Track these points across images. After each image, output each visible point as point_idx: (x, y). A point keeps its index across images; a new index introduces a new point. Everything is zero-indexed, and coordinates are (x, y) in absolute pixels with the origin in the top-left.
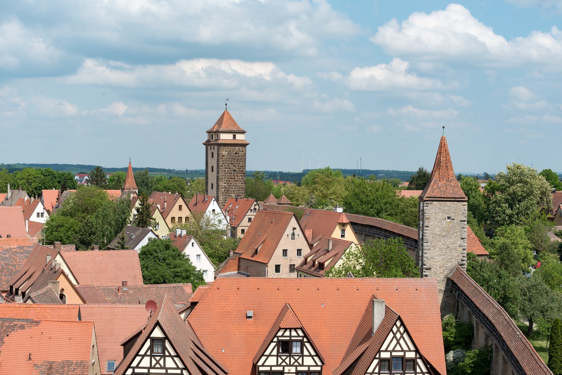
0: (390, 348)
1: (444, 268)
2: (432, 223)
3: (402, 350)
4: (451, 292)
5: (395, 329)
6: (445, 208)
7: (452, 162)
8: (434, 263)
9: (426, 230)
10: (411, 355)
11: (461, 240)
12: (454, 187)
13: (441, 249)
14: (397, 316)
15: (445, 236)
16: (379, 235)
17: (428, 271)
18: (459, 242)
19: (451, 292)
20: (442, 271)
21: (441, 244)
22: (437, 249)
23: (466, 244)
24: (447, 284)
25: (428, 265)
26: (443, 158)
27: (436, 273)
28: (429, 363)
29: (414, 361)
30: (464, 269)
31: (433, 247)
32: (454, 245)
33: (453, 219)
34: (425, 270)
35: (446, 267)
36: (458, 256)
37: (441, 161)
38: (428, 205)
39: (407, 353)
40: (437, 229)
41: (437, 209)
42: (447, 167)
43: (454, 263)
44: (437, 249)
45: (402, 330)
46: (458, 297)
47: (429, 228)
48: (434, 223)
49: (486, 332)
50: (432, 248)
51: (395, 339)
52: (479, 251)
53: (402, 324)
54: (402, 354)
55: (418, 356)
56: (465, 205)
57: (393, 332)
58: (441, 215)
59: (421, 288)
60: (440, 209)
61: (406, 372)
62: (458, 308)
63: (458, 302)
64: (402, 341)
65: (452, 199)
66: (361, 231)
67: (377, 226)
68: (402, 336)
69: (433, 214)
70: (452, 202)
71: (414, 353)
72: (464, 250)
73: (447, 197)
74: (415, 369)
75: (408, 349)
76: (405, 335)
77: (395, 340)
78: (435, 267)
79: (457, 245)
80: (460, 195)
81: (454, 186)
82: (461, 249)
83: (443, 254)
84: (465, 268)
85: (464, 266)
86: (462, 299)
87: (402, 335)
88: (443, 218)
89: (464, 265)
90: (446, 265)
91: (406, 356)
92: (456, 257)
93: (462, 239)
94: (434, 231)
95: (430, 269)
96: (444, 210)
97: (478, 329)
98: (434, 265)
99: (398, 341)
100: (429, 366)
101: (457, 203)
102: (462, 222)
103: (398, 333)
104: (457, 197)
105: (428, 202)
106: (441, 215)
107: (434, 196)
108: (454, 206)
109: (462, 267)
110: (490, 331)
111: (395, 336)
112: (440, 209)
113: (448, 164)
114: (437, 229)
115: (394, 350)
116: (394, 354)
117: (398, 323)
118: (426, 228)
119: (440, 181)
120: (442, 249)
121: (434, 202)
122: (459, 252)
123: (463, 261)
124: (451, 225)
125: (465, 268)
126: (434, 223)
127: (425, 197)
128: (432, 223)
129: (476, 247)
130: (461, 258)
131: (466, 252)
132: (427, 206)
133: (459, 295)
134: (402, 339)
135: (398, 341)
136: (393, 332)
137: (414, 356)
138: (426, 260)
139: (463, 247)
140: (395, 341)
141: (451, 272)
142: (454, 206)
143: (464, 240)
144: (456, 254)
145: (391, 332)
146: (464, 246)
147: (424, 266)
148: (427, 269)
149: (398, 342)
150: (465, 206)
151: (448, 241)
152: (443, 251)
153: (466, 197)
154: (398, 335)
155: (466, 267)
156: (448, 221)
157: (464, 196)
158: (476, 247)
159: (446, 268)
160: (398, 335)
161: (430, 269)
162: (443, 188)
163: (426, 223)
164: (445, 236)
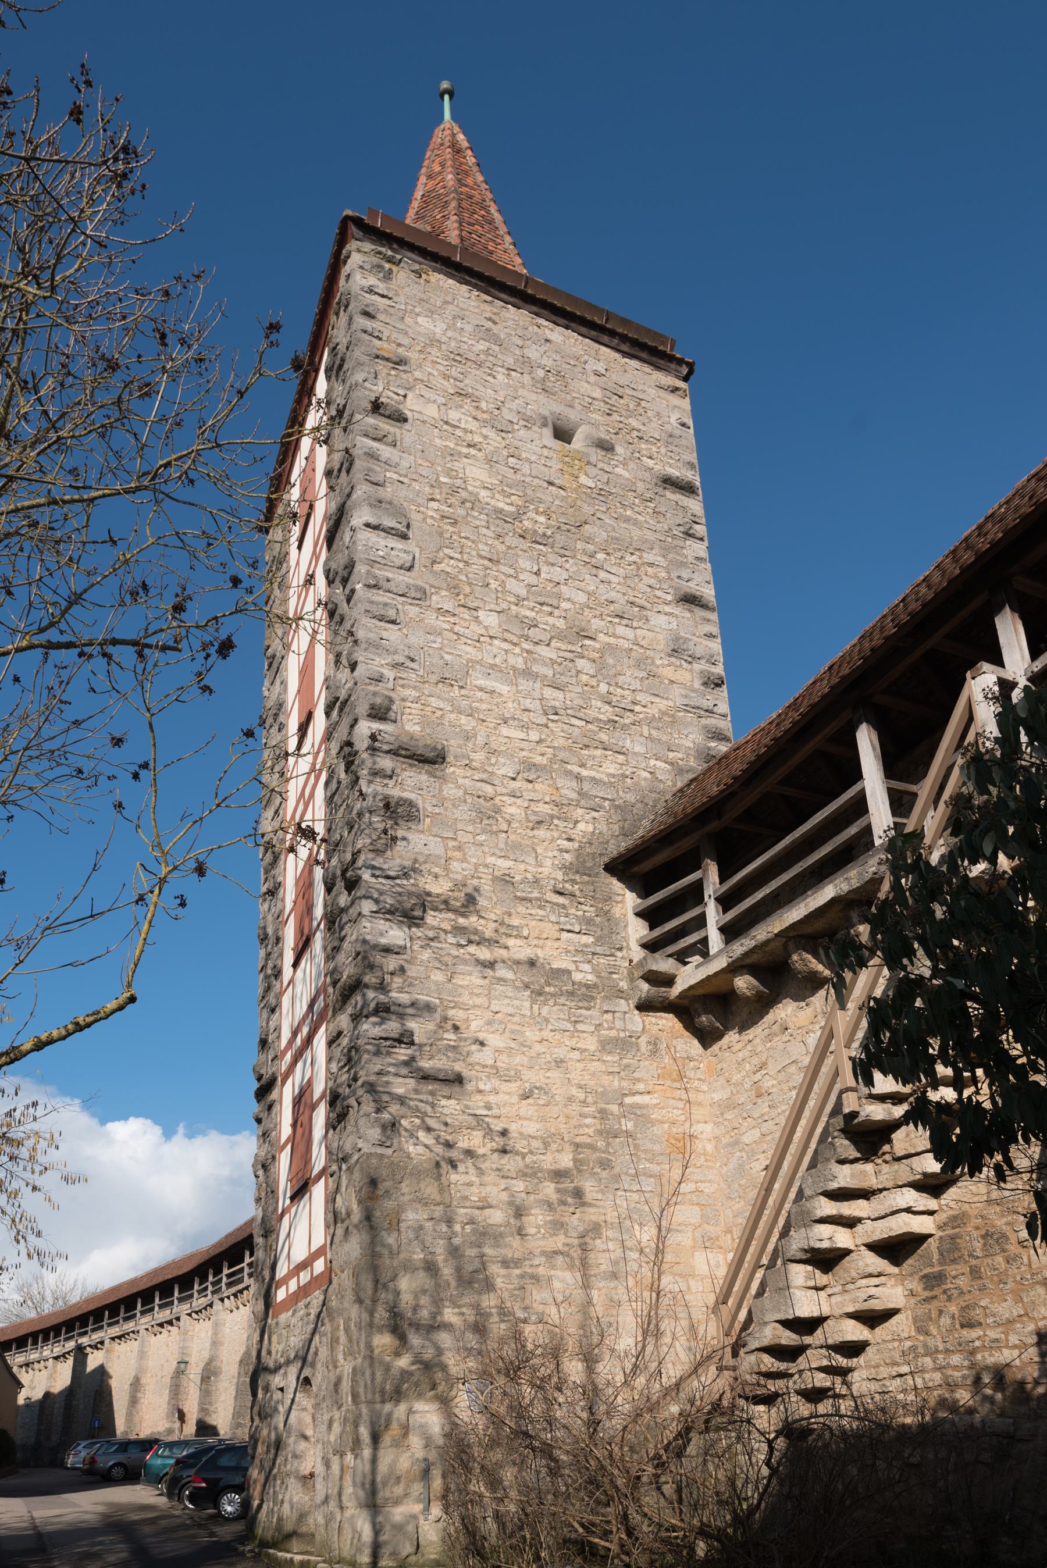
11: (678, 610)
20: (547, 809)
22: (491, 620)
31: (455, 590)
32: (629, 633)
35: (578, 778)
41: (469, 328)
48: (454, 415)
78: (479, 757)
83: (550, 673)
90: (576, 769)
92: (651, 721)
132: (388, 276)
139: (697, 667)
143: (700, 613)
159: (581, 793)
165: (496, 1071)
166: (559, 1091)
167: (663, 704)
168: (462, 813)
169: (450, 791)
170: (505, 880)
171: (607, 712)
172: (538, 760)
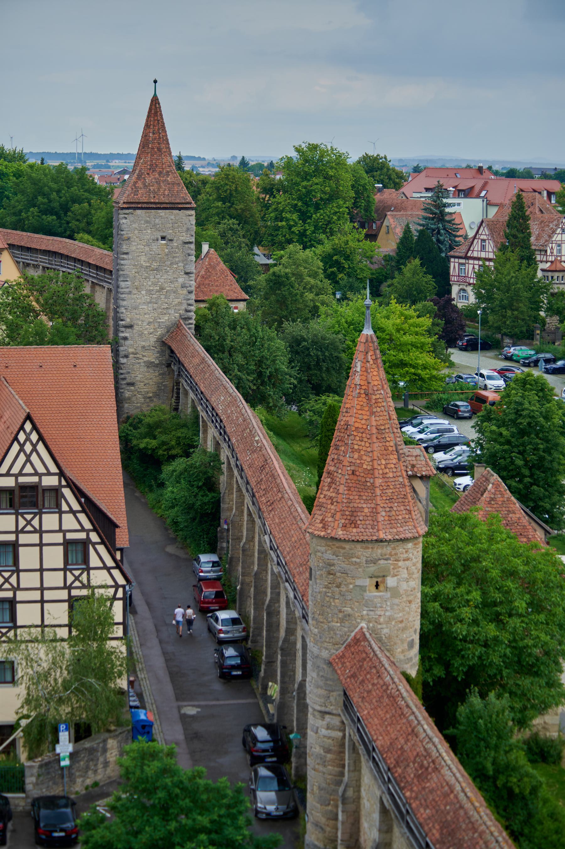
0: (15, 470)
1: (156, 325)
2: (134, 248)
3: (36, 473)
4: (169, 366)
5: (22, 437)
6: (157, 221)
7: (170, 141)
8: (138, 316)
9: (123, 259)
10: (51, 481)
11: (185, 276)
12: (173, 184)
13: (149, 292)
14: (25, 414)
15: (157, 269)
16: (65, 267)
17: (128, 330)
18: (181, 280)
19: (169, 366)
20: (152, 330)
21: (150, 283)
22: (143, 292)
23: (193, 283)
24: (162, 353)
25: (128, 320)
26: (154, 134)
27: (141, 334)
28: (83, 494)
29: (56, 491)
30: (191, 326)
31: (137, 288)
32: (173, 286)
33: (171, 240)
34: (123, 329)
36: (180, 303)
37: (151, 139)
38: (126, 216)
39: (43, 478)
40: (143, 258)
41: (143, 222)
42: (159, 150)
43: (173, 316)
44: (143, 292)
45: (34, 437)
46: (179, 375)
47: (130, 256)
48: (138, 247)
49: (215, 435)
50: (135, 291)
51: (22, 454)
52: (231, 293)
53: (35, 427)
54: (35, 479)
55: (64, 483)
56: (192, 215)
57: (19, 442)
58: (149, 234)
59: (83, 363)
60: (147, 222)
61: (44, 510)
62: (178, 393)
63: (178, 383)
64: (34, 458)
65: (168, 206)
66: (37, 261)
67: (61, 251)
68: (34, 449)
69: (136, 232)
70: (167, 211)
71: (57, 477)
72: (190, 292)
73: (161, 201)
74: (58, 505)
75: (45, 471)
76: (41, 447)
77: (22, 456)
78: (140, 323)
79: (178, 285)
80: (183, 197)
81: (173, 184)
82: (185, 292)
84: (192, 324)
85: (190, 321)
86: (184, 379)
87: (34, 446)
88: (152, 237)
89: (190, 319)
91: (43, 484)
92: (176, 305)
93: (187, 273)
94: (138, 261)
95: (131, 327)
96: (155, 225)
97: (205, 431)
98: (138, 319)
99: (28, 457)
100: (83, 500)
101: (177, 211)
102: (186, 246)
103: (34, 442)
104: (178, 201)
105: (127, 211)
106: (149, 234)
107: (137, 201)
108: (173, 217)
109: (187, 322)
110: (221, 434)
111: (22, 449)
112: (147, 222)
113: (163, 146)
114: (143, 258)
115: (21, 474)
116: (21, 479)
117: (28, 426)
118: (125, 256)
119: (148, 174)
120: (152, 292)
121: (139, 212)
122: (182, 296)
123: (190, 311)
124: (167, 250)
125: (192, 324)
126: (138, 247)
127: (122, 202)
128: (134, 248)
129: (227, 287)
130: (184, 306)
131: (193, 297)
132: (126, 218)
133: (179, 372)
134: (34, 454)
135: (28, 457)
136: (19, 442)
137: (56, 483)
138: (124, 311)
140: (22, 458)
141: (168, 332)
142: (173, 217)
144: (177, 301)
145: (16, 442)
146: (190, 286)
147: (121, 323)
148: (126, 327)
149: (28, 460)
150: (191, 218)
151: (163, 278)
152: (154, 296)
153: (193, 202)
154: (28, 448)
155: (194, 322)
156: (162, 244)
157: (189, 198)
158: (227, 287)
160: (28, 448)
161: (131, 327)
162: (153, 186)
163: (124, 247)
164: (157, 269)
165: (140, 382)
166: (151, 383)
167: (179, 300)
168: (137, 335)
169: (135, 331)
170: (143, 347)
171: (166, 306)
172: (151, 320)
